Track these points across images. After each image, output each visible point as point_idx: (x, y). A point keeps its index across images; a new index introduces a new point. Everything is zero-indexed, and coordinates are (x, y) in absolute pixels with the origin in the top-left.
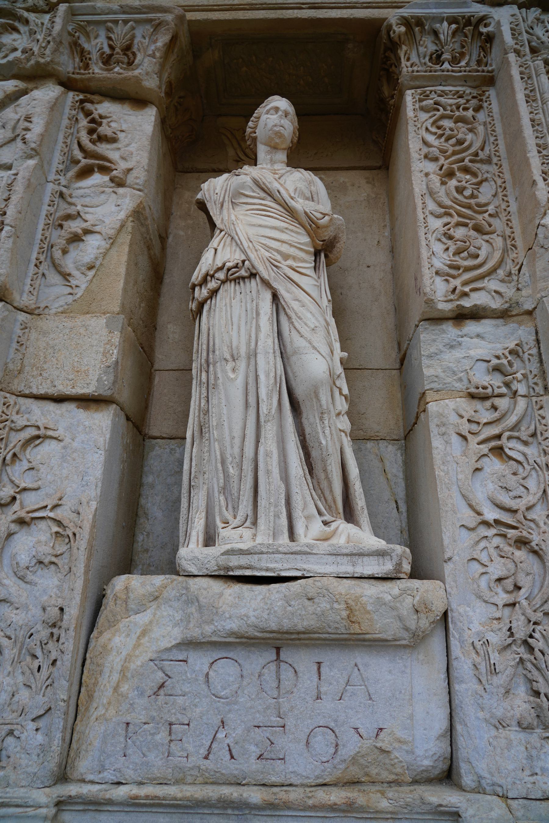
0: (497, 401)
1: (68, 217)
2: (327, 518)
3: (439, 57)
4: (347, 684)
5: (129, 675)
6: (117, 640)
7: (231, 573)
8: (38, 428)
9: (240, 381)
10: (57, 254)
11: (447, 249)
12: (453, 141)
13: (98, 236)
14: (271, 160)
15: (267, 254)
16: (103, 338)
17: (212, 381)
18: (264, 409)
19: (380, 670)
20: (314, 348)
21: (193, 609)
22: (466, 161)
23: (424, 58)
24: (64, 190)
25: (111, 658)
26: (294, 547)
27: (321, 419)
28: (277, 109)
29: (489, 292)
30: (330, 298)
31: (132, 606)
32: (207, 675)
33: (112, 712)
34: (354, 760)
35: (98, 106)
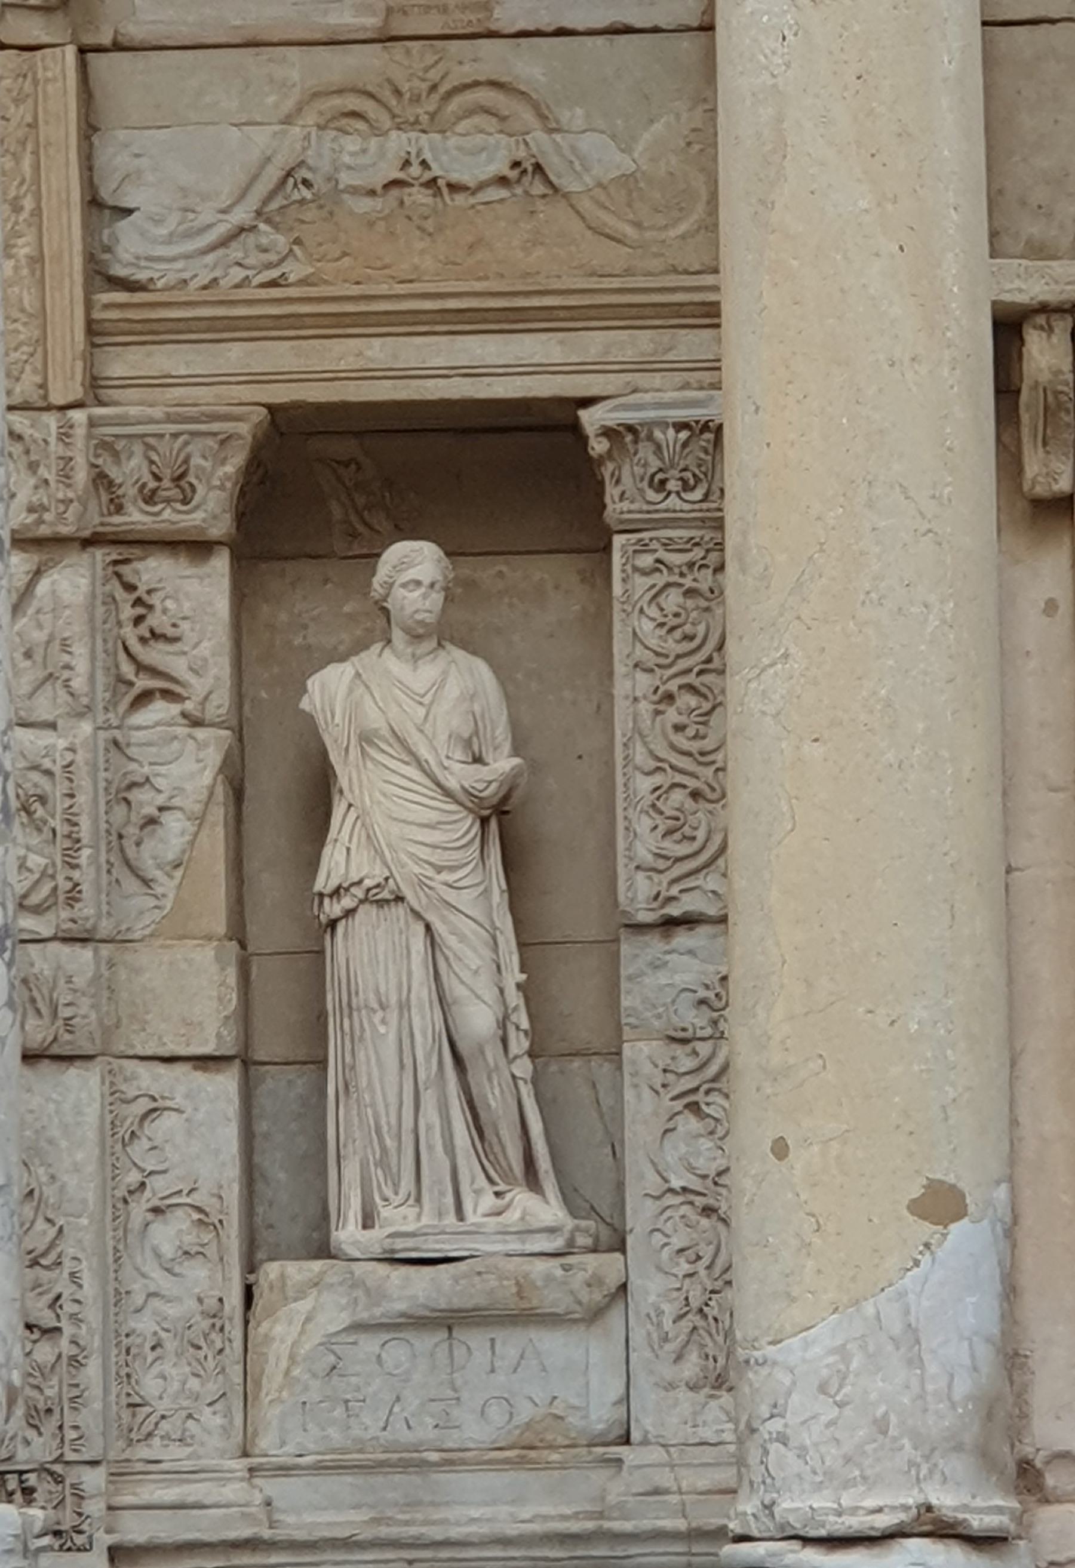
0: (699, 1046)
1: (133, 785)
2: (502, 1187)
3: (663, 482)
4: (522, 1357)
5: (299, 1359)
6: (279, 1329)
7: (397, 1256)
8: (154, 1099)
9: (392, 1037)
10: (131, 852)
11: (656, 827)
12: (678, 634)
13: (179, 814)
14: (413, 655)
15: (417, 870)
16: (216, 978)
17: (358, 1033)
18: (422, 1076)
19: (553, 1343)
20: (478, 997)
21: (359, 1293)
22: (693, 674)
23: (642, 479)
24: (117, 734)
25: (275, 1345)
26: (462, 1227)
27: (490, 1079)
28: (418, 583)
29: (705, 892)
30: (504, 886)
31: (290, 1294)
32: (379, 1356)
33: (285, 1394)
34: (528, 1425)
35: (138, 565)
